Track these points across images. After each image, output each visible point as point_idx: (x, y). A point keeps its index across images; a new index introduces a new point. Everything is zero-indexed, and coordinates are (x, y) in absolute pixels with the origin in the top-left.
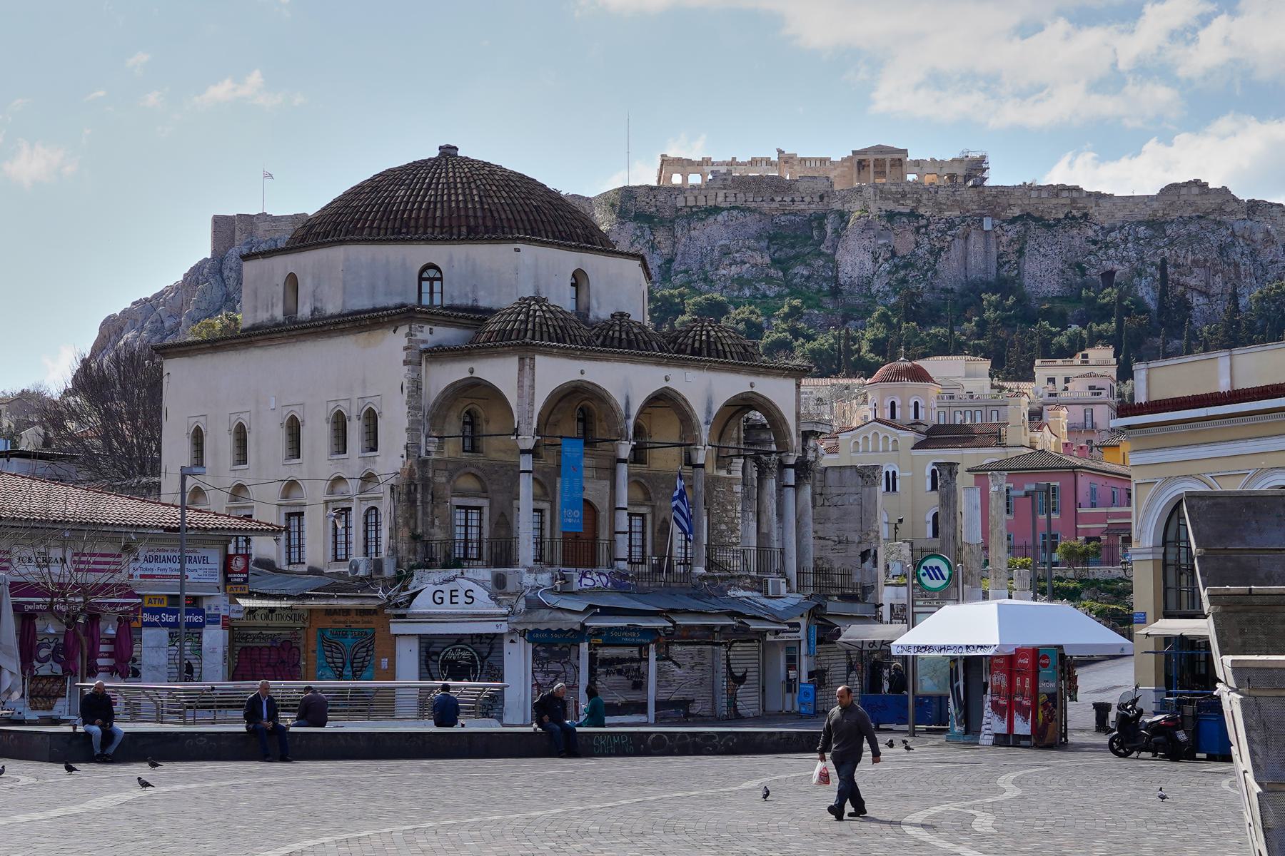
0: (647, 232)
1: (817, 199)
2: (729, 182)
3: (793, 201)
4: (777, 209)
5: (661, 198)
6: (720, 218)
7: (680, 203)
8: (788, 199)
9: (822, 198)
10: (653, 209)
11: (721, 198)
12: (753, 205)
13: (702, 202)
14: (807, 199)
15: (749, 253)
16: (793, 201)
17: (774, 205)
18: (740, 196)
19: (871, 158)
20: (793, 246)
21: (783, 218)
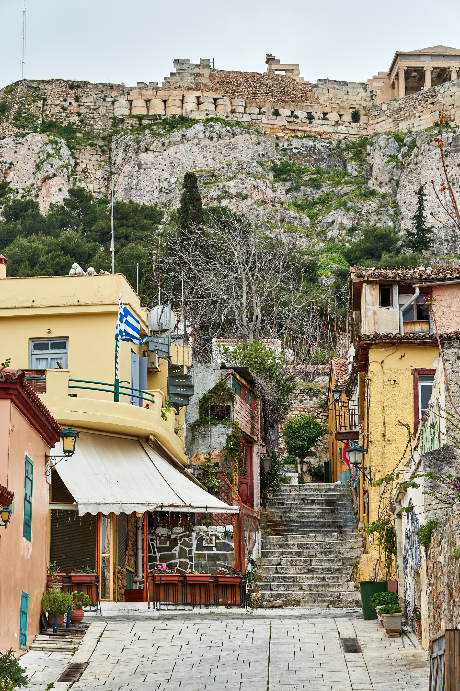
0: (65, 151)
1: (347, 117)
2: (205, 80)
3: (310, 117)
4: (284, 129)
5: (88, 101)
6: (190, 133)
7: (121, 109)
8: (302, 114)
9: (356, 117)
10: (74, 119)
11: (190, 105)
12: (245, 118)
13: (157, 109)
14: (333, 116)
15: (251, 181)
16: (310, 117)
17: (280, 122)
18: (224, 102)
19: (429, 65)
20: (316, 185)
21: (295, 143)
